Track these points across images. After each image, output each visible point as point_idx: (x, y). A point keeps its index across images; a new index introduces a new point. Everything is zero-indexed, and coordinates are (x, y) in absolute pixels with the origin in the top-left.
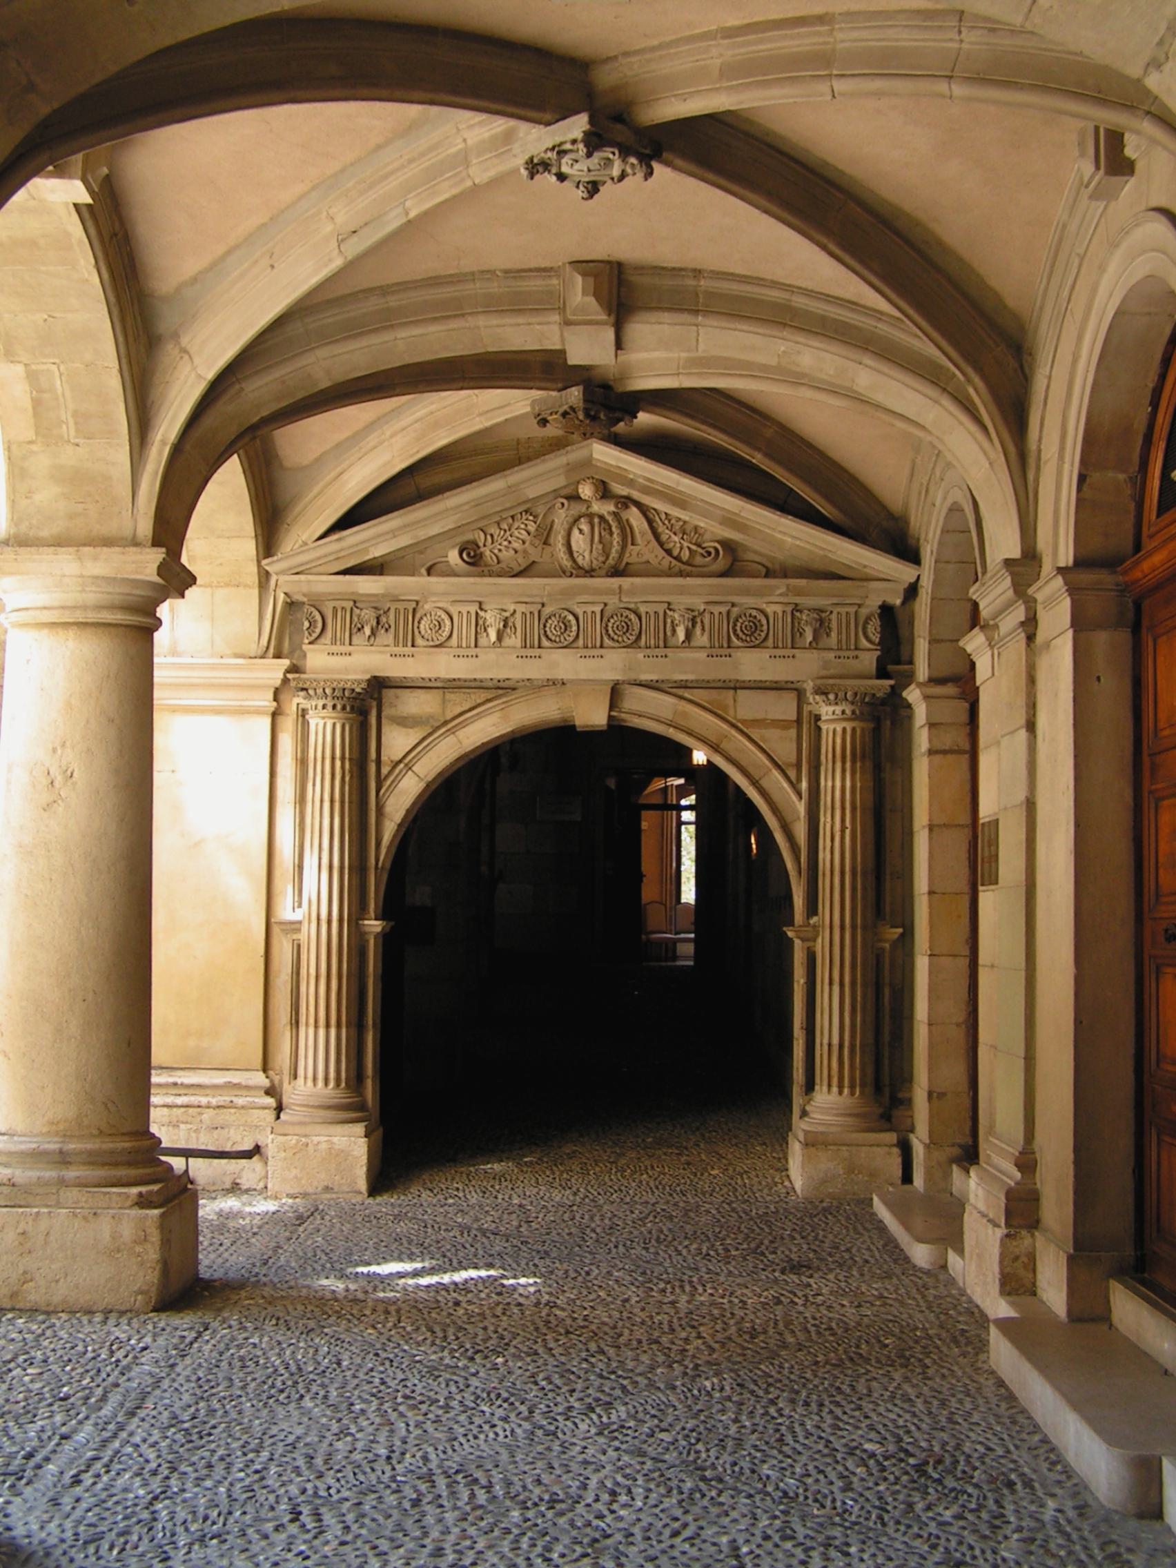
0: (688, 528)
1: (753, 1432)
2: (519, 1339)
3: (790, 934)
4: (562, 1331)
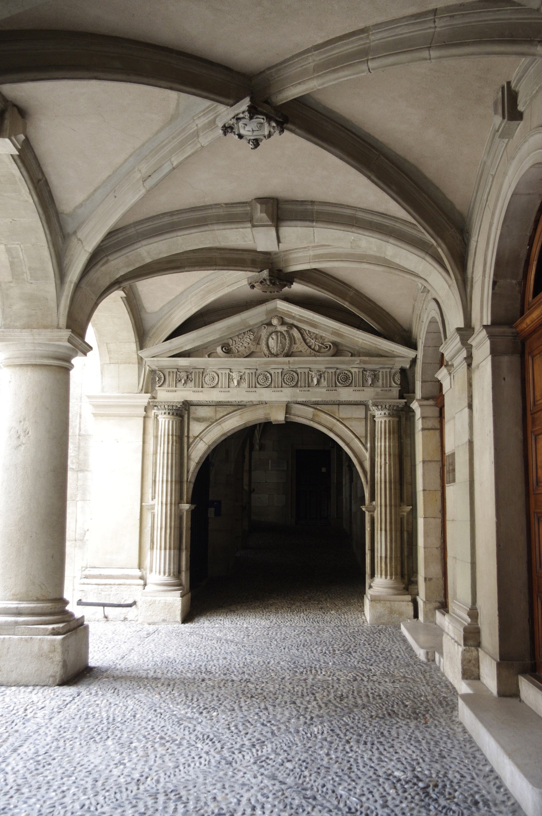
0: (318, 337)
1: (337, 762)
2: (228, 700)
3: (364, 509)
4: (250, 696)
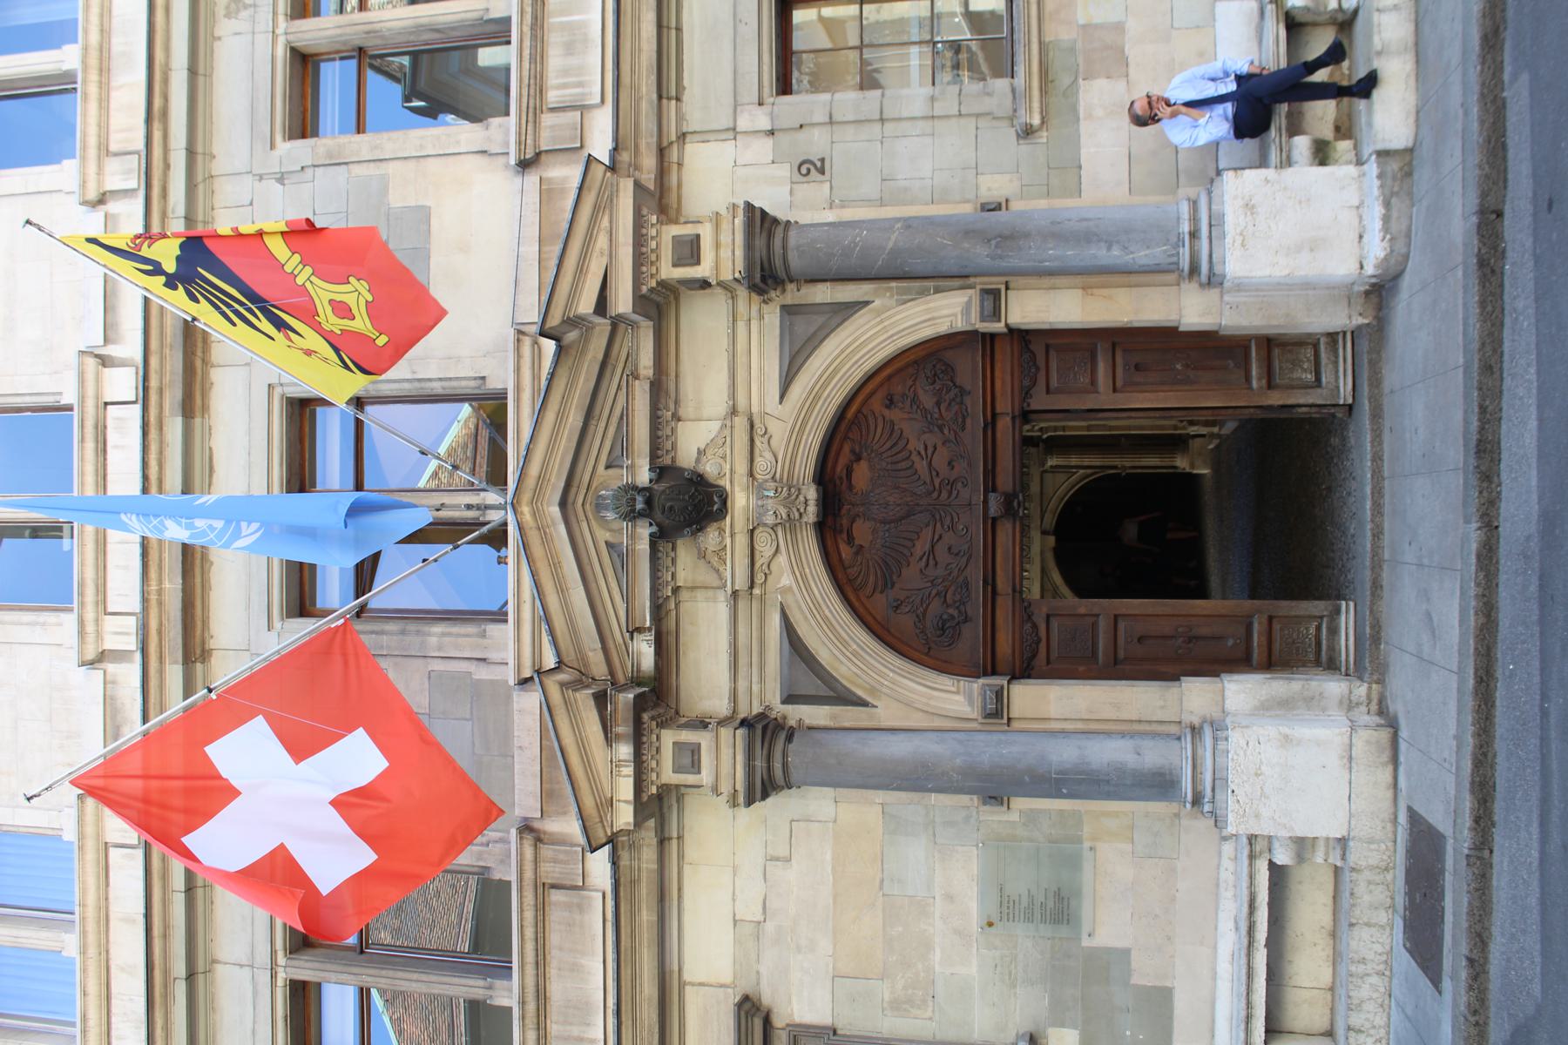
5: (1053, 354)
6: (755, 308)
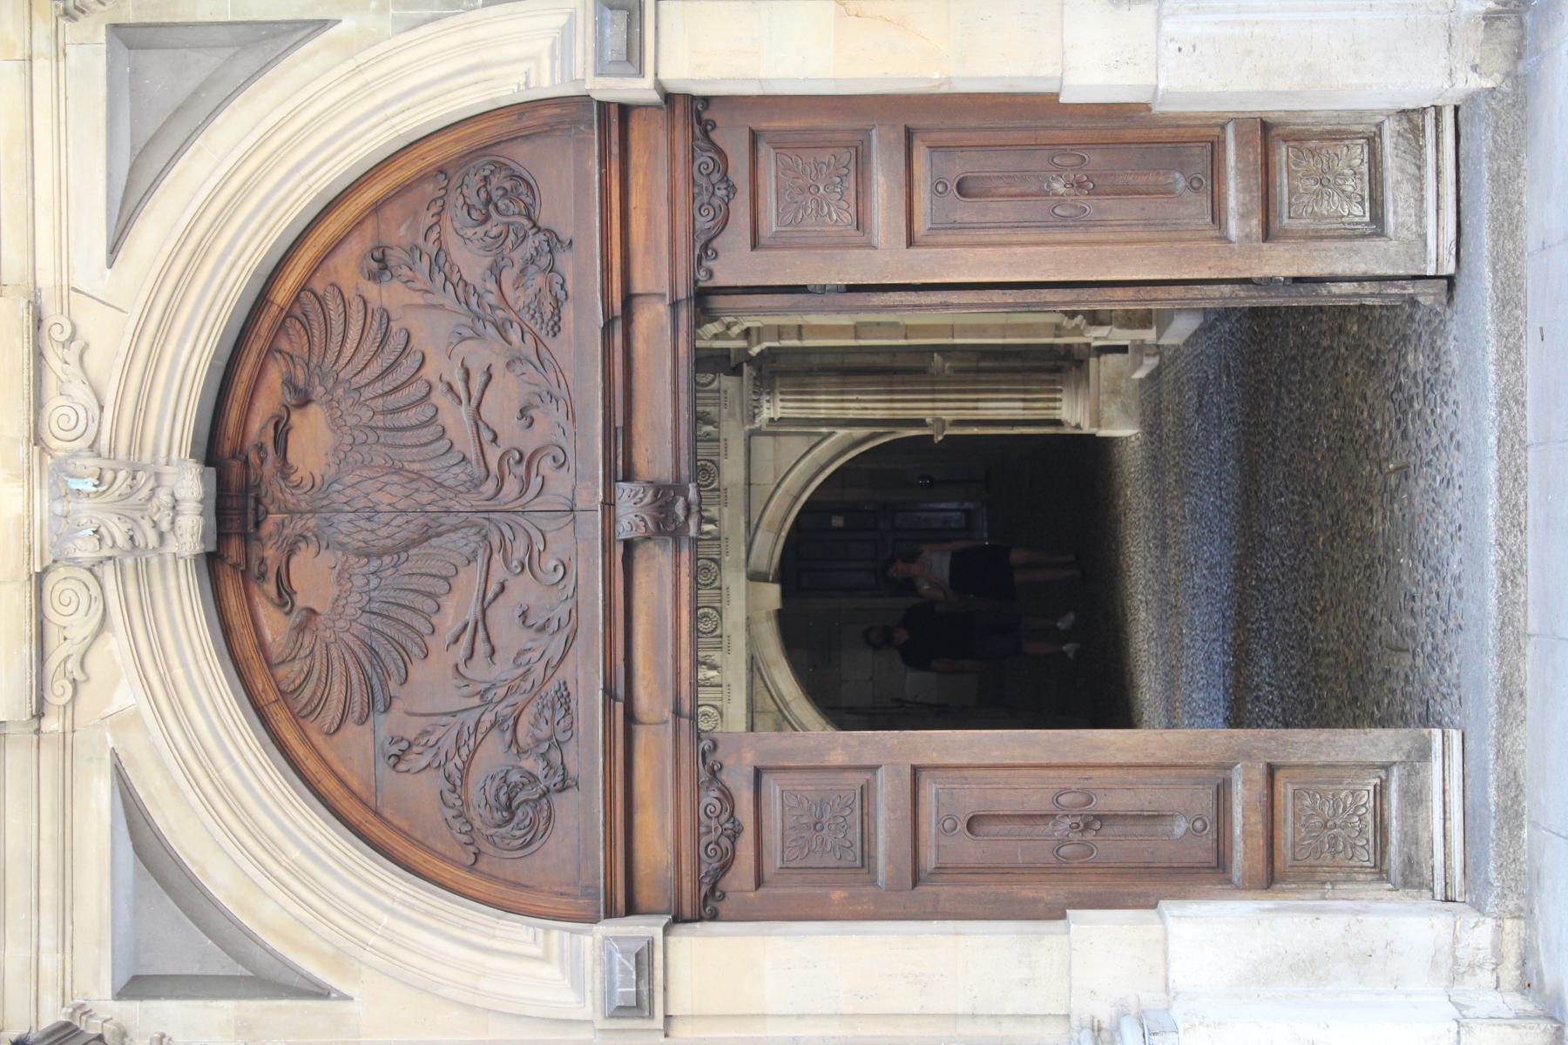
3: (940, 438)
5: (766, 153)
6: (43, 29)
